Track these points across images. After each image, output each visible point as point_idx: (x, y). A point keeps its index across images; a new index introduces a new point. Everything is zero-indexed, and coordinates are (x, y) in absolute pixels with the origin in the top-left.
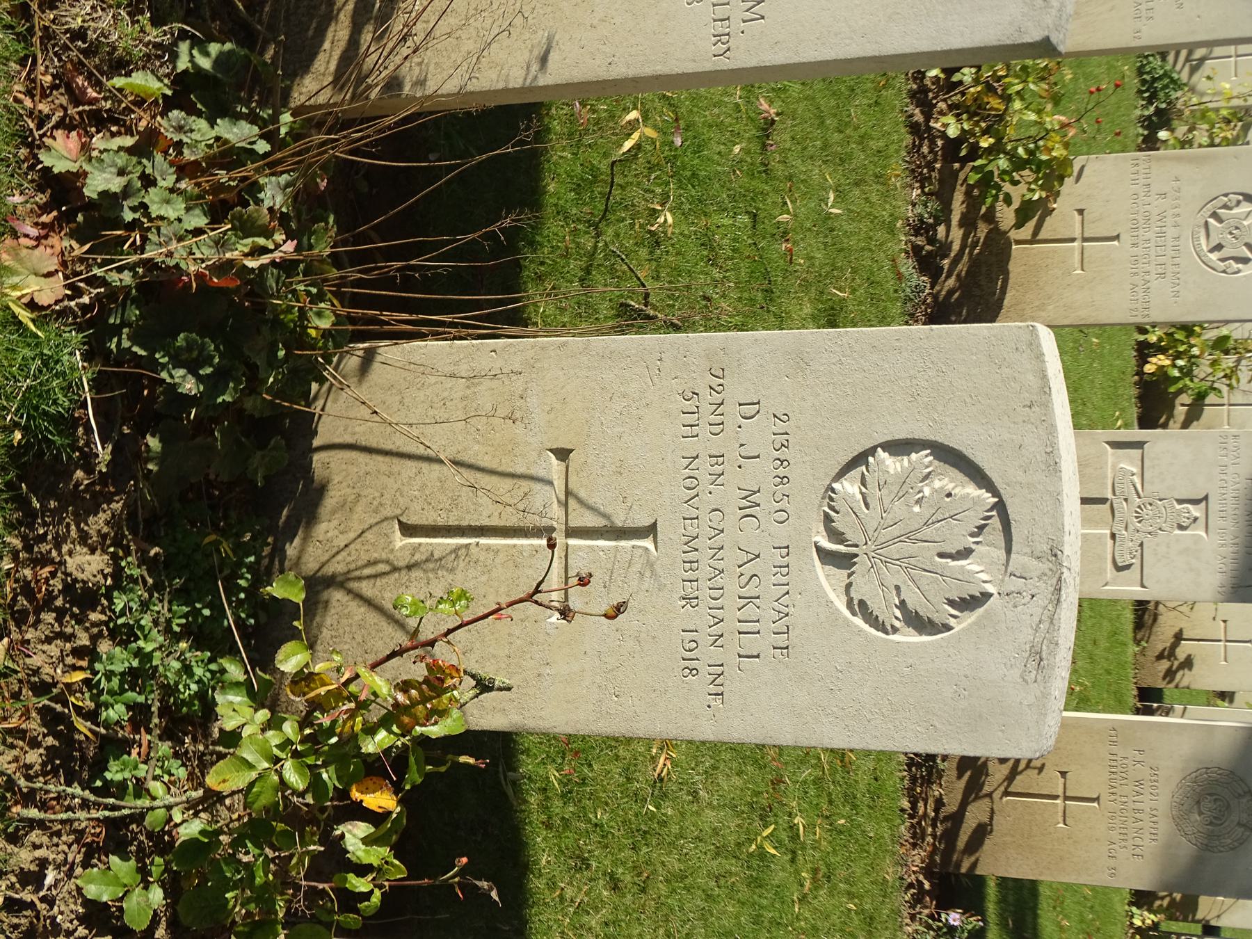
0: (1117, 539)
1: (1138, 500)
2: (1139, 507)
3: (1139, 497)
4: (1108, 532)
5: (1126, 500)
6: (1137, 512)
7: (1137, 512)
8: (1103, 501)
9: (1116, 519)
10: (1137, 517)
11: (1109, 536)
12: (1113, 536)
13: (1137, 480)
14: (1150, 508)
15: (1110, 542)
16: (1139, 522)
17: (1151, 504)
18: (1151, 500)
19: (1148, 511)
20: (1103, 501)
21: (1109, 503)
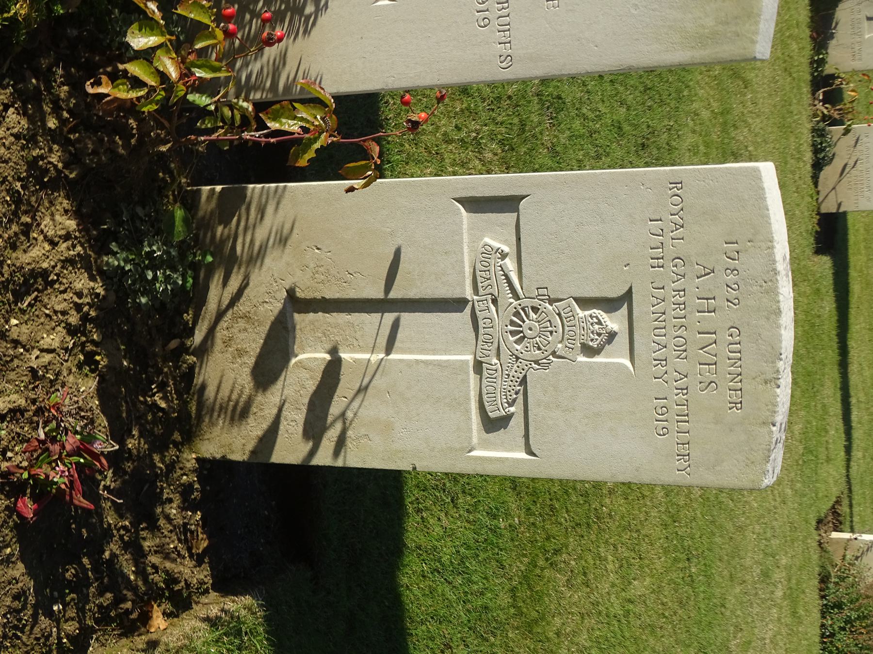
0: (485, 373)
1: (515, 303)
2: (517, 314)
3: (516, 297)
4: (470, 358)
5: (495, 301)
6: (512, 323)
7: (512, 323)
8: (457, 304)
9: (481, 337)
10: (513, 333)
11: (471, 364)
12: (478, 366)
13: (510, 264)
14: (532, 314)
15: (473, 377)
16: (518, 342)
17: (535, 309)
18: (536, 302)
19: (531, 323)
20: (457, 304)
21: (468, 310)
